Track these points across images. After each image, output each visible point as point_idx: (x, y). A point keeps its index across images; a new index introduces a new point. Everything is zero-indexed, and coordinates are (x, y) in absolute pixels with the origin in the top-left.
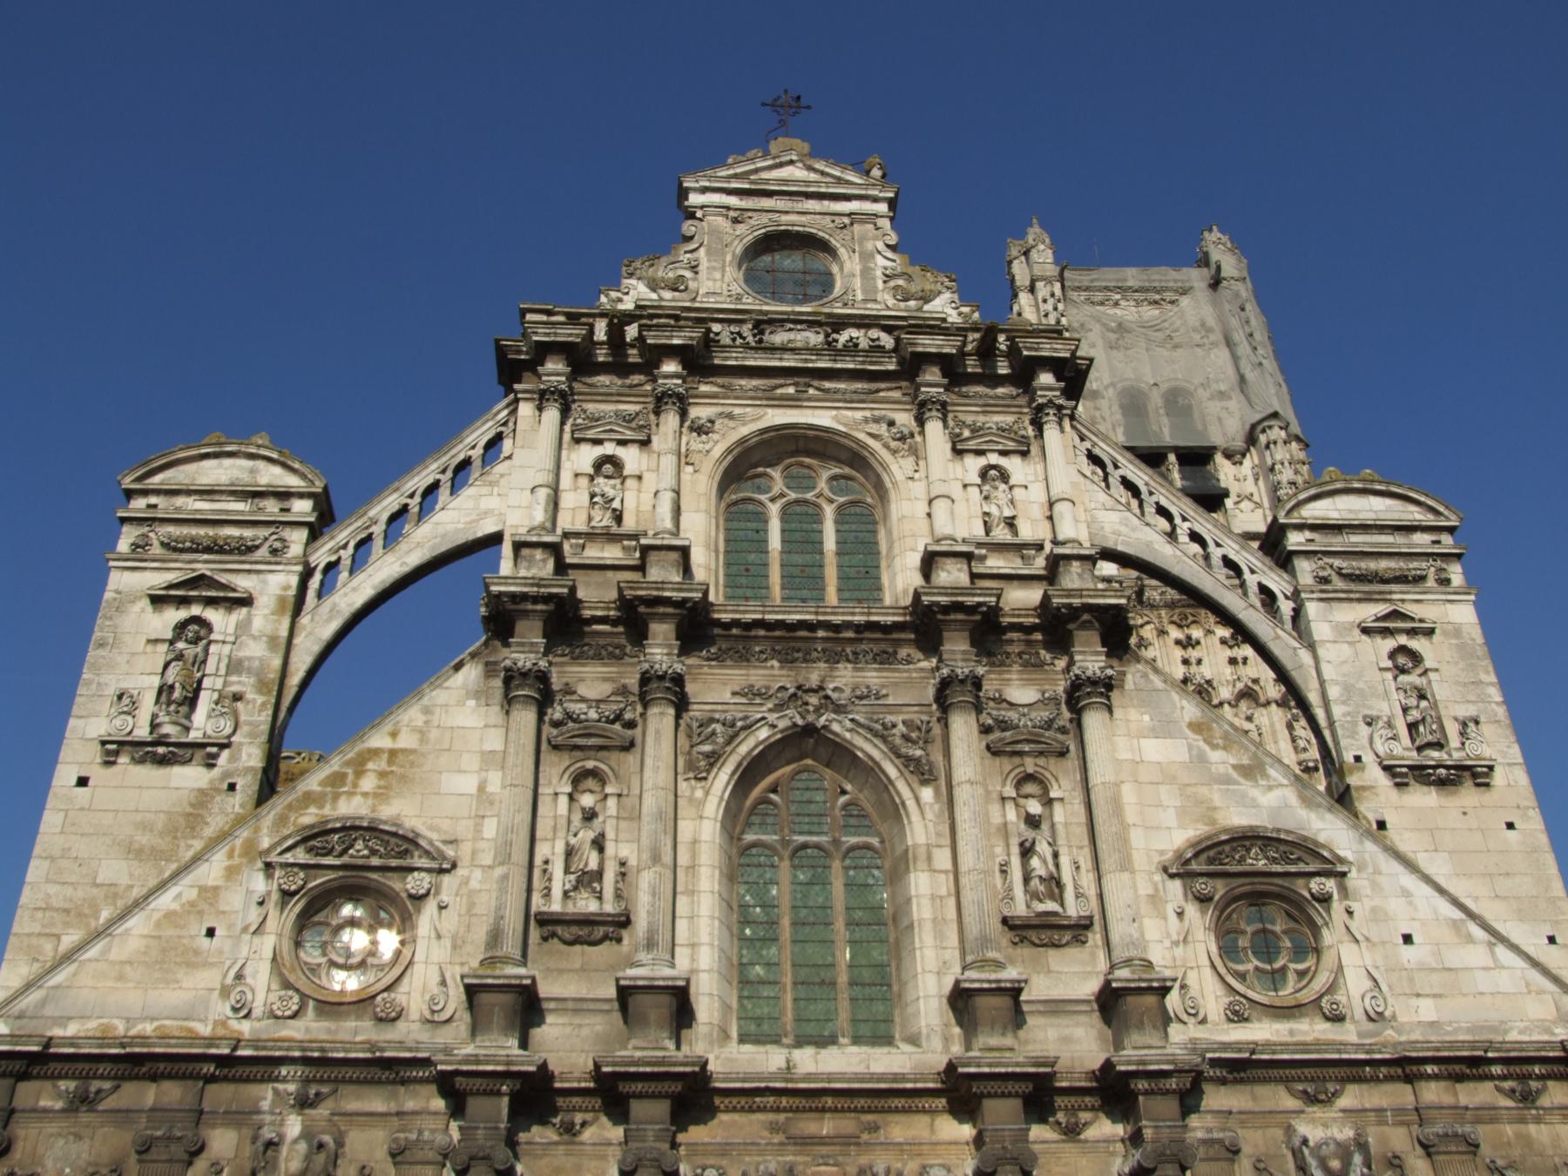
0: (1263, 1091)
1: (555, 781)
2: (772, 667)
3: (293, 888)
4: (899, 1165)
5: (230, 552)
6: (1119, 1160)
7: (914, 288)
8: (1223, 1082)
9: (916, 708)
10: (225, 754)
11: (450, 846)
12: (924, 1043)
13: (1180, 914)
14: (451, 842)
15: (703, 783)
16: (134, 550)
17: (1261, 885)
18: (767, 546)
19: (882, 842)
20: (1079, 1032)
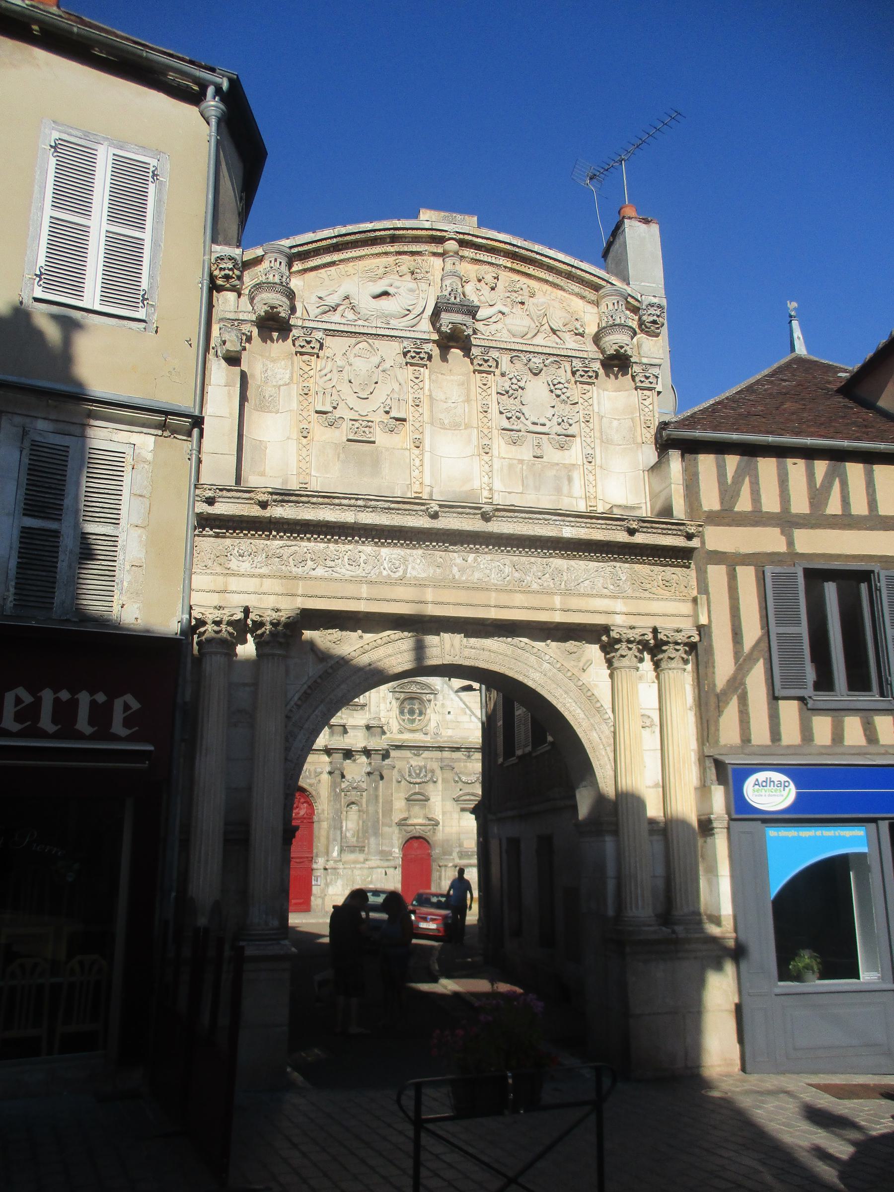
8: (394, 749)
13: (390, 703)
17: (413, 695)
20: (359, 734)
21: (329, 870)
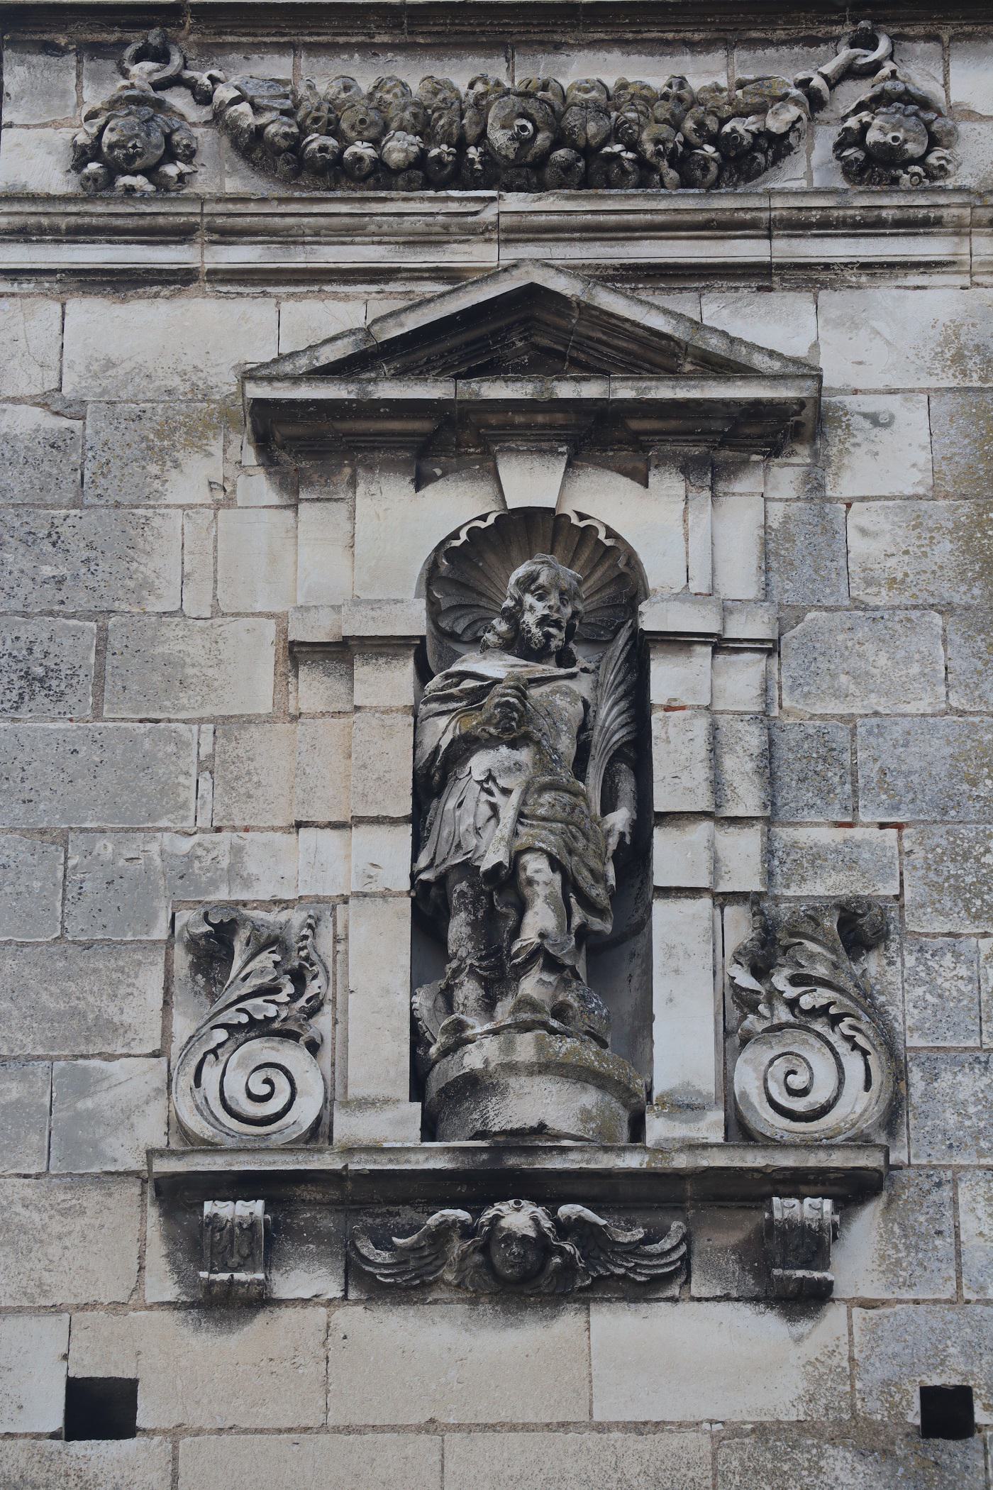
5: (645, 175)
10: (869, 1219)
16: (100, 187)
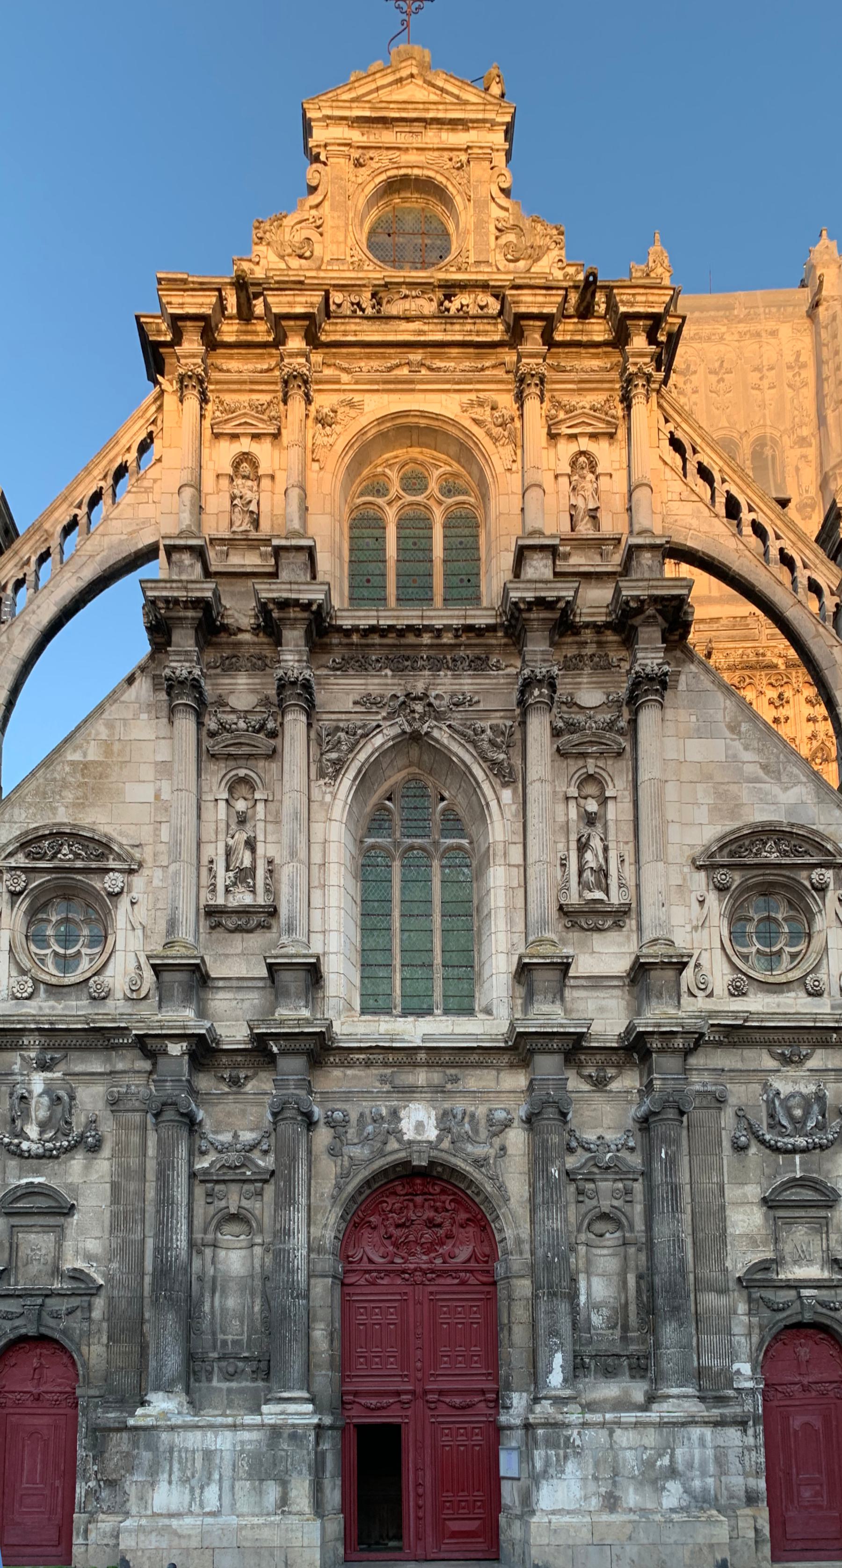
0: (749, 1053)
1: (214, 788)
2: (386, 675)
3: (18, 889)
4: (473, 1109)
6: (634, 1107)
7: (526, 241)
9: (502, 714)
11: (136, 849)
12: (495, 1012)
14: (137, 846)
15: (331, 789)
18: (385, 555)
19: (471, 843)
21: (540, 1431)
